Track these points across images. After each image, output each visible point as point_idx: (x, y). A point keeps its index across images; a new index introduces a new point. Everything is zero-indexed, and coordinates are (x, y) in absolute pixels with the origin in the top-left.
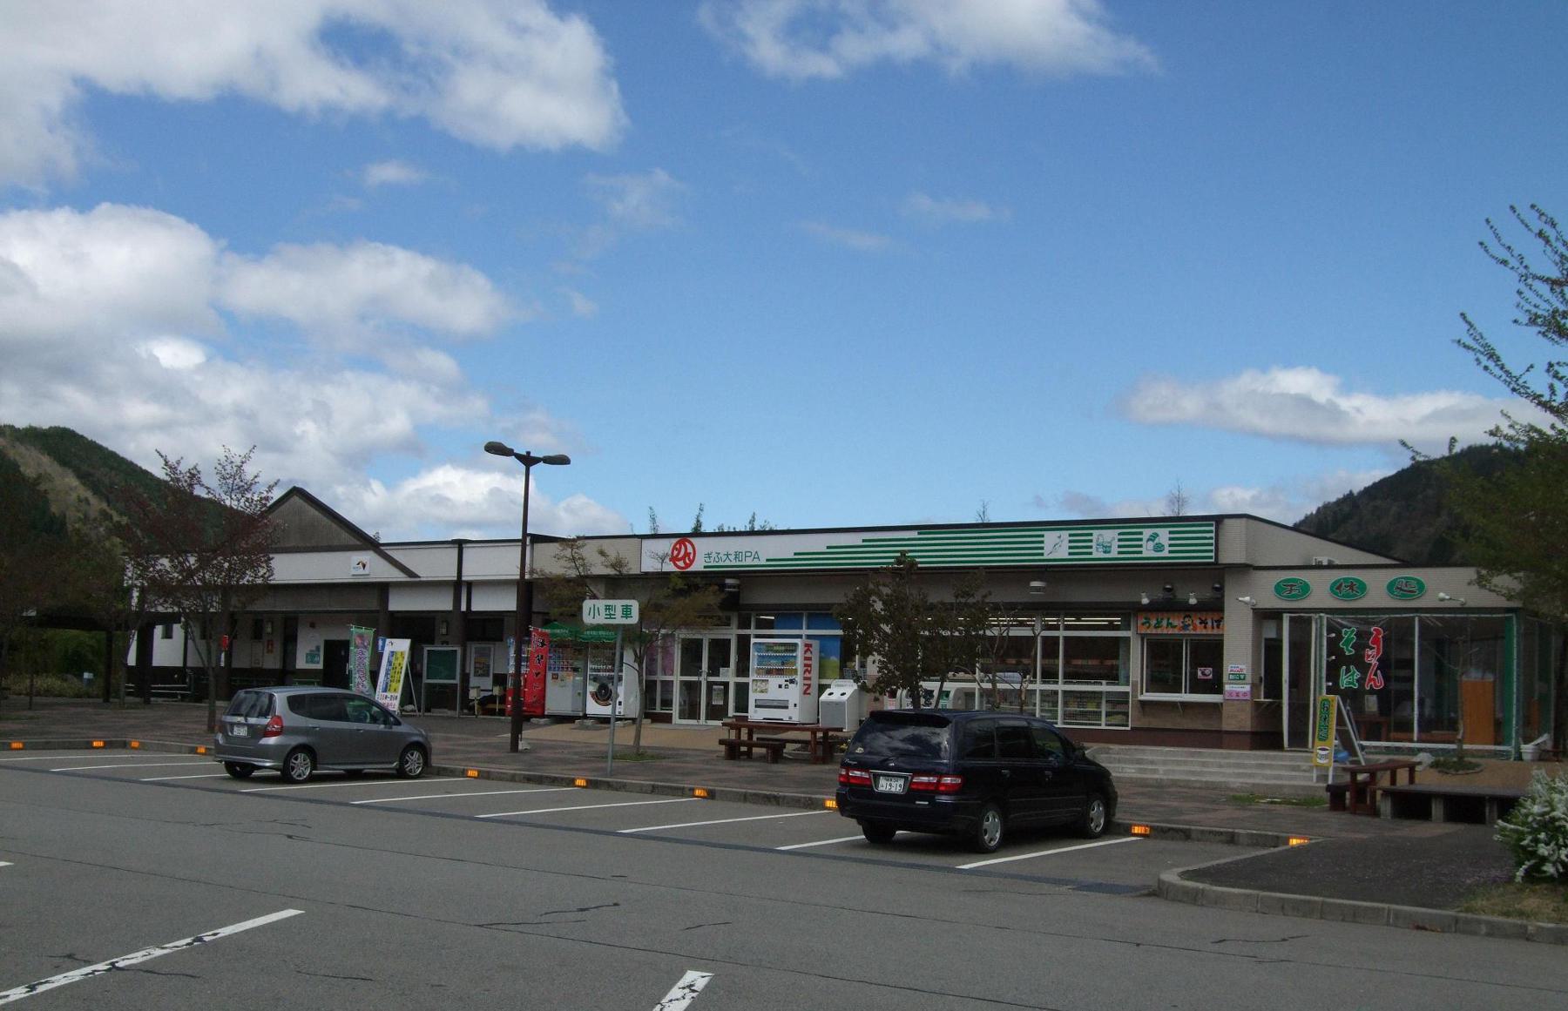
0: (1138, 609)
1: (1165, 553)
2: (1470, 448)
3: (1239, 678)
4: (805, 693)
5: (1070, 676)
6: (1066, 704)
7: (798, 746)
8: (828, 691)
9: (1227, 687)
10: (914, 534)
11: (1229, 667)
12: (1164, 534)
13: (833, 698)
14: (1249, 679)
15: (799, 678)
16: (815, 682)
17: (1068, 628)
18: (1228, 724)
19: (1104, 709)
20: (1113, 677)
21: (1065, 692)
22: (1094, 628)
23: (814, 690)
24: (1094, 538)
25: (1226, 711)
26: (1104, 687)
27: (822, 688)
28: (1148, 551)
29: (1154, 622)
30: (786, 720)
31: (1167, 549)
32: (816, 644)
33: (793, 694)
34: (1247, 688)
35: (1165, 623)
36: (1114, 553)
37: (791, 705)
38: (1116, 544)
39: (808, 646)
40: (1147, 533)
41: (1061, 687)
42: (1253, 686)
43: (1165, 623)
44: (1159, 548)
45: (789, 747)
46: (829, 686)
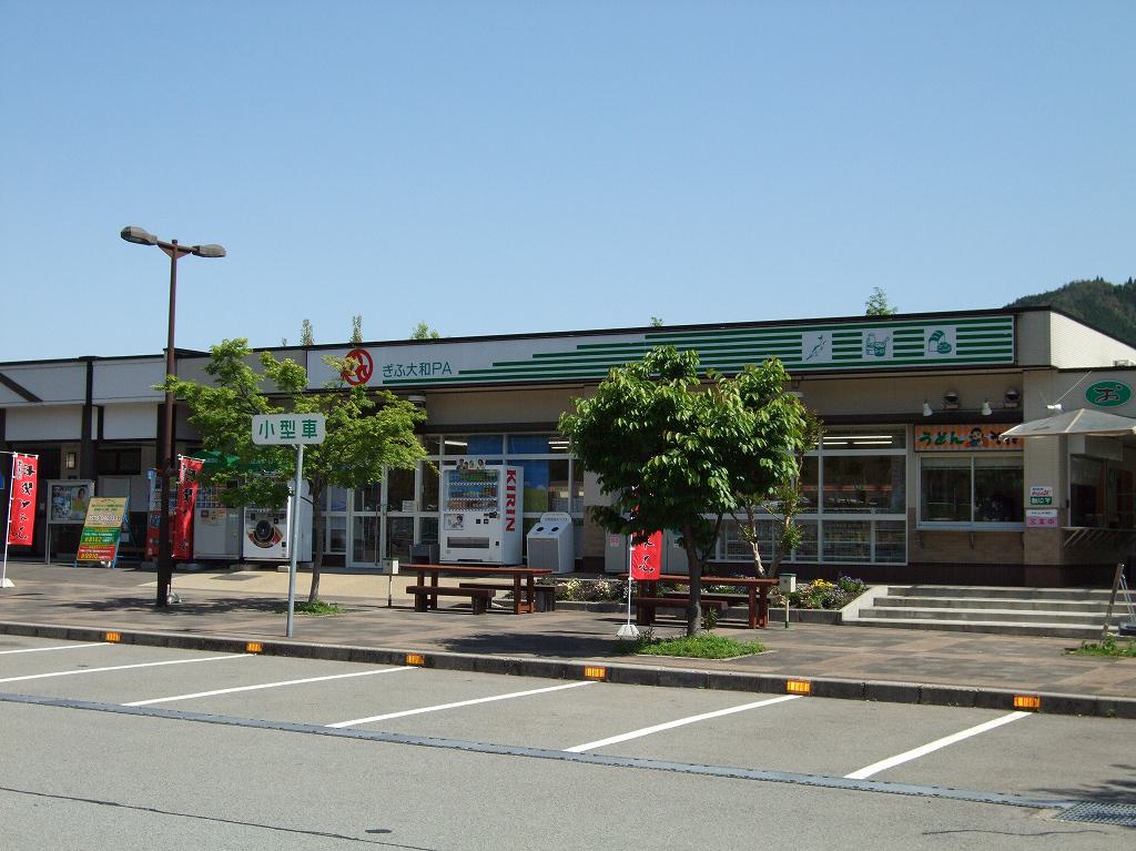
0: (917, 420)
1: (952, 355)
2: (1072, 284)
3: (1045, 502)
4: (508, 529)
5: (830, 506)
6: (826, 535)
7: (507, 592)
8: (537, 526)
9: (1029, 513)
10: (641, 338)
11: (1031, 489)
12: (950, 333)
13: (542, 535)
14: (1056, 502)
15: (502, 512)
16: (519, 516)
17: (826, 447)
18: (1032, 557)
19: (873, 542)
20: (882, 504)
21: (825, 522)
22: (875, 443)
23: (518, 526)
24: (864, 338)
25: (1027, 539)
26: (873, 517)
27: (528, 524)
28: (931, 352)
29: (934, 437)
30: (486, 560)
31: (955, 349)
32: (519, 470)
33: (495, 530)
34: (1054, 513)
35: (948, 438)
36: (889, 356)
37: (492, 544)
38: (891, 344)
39: (511, 473)
40: (929, 331)
41: (820, 516)
42: (1061, 511)
43: (948, 438)
44: (944, 348)
45: (500, 595)
46: (538, 520)
